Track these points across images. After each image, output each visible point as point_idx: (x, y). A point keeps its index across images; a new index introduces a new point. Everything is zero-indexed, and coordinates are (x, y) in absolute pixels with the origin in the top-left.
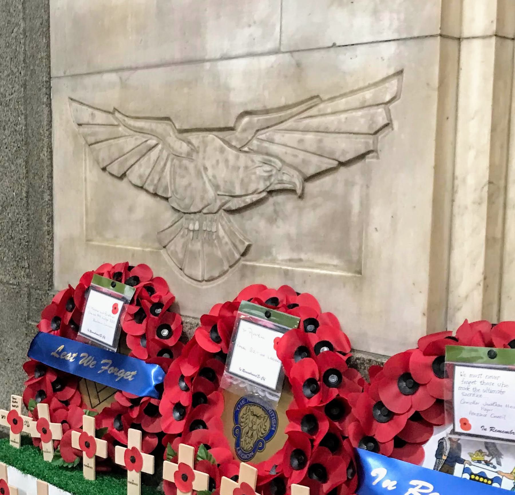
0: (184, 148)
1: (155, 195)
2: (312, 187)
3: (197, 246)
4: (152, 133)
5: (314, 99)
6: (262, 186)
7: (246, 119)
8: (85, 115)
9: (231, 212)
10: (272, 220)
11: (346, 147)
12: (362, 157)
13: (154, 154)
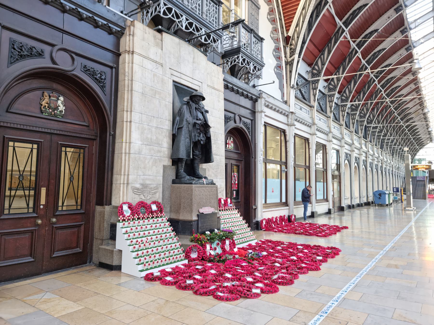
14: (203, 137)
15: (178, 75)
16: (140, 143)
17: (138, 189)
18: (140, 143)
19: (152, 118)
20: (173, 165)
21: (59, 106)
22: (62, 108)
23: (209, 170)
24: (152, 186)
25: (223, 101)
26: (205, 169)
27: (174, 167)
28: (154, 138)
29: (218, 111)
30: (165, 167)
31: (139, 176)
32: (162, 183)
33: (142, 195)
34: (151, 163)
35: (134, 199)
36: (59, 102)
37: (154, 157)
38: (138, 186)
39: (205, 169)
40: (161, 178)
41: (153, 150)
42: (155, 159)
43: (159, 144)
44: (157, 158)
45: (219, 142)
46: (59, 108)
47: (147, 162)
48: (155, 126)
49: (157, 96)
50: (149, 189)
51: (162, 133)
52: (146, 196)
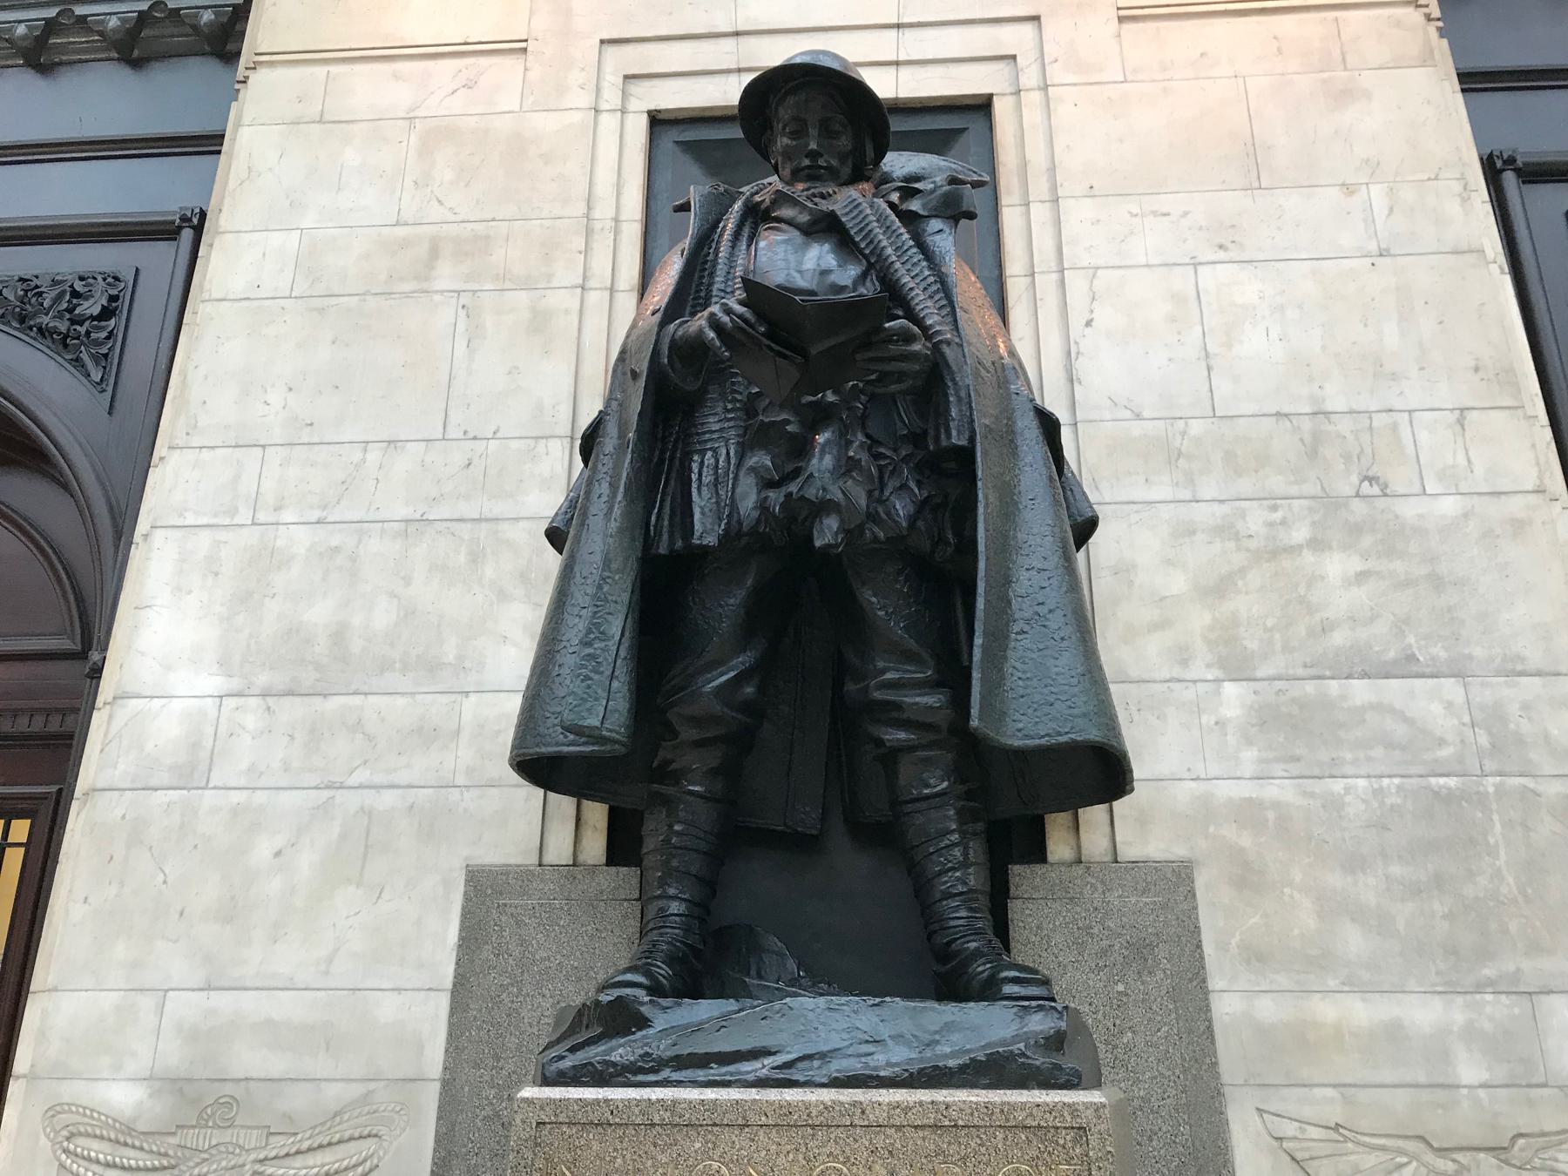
7: (1521, 1141)
14: (847, 467)
16: (213, 683)
18: (213, 683)
23: (1248, 878)
24: (297, 1101)
25: (1460, 96)
27: (627, 876)
28: (383, 616)
29: (1349, 189)
30: (484, 889)
31: (147, 1002)
34: (306, 861)
37: (352, 800)
38: (122, 1097)
41: (357, 726)
42: (367, 812)
43: (433, 667)
44: (388, 799)
47: (263, 849)
49: (446, 275)
50: (253, 1139)
51: (476, 558)
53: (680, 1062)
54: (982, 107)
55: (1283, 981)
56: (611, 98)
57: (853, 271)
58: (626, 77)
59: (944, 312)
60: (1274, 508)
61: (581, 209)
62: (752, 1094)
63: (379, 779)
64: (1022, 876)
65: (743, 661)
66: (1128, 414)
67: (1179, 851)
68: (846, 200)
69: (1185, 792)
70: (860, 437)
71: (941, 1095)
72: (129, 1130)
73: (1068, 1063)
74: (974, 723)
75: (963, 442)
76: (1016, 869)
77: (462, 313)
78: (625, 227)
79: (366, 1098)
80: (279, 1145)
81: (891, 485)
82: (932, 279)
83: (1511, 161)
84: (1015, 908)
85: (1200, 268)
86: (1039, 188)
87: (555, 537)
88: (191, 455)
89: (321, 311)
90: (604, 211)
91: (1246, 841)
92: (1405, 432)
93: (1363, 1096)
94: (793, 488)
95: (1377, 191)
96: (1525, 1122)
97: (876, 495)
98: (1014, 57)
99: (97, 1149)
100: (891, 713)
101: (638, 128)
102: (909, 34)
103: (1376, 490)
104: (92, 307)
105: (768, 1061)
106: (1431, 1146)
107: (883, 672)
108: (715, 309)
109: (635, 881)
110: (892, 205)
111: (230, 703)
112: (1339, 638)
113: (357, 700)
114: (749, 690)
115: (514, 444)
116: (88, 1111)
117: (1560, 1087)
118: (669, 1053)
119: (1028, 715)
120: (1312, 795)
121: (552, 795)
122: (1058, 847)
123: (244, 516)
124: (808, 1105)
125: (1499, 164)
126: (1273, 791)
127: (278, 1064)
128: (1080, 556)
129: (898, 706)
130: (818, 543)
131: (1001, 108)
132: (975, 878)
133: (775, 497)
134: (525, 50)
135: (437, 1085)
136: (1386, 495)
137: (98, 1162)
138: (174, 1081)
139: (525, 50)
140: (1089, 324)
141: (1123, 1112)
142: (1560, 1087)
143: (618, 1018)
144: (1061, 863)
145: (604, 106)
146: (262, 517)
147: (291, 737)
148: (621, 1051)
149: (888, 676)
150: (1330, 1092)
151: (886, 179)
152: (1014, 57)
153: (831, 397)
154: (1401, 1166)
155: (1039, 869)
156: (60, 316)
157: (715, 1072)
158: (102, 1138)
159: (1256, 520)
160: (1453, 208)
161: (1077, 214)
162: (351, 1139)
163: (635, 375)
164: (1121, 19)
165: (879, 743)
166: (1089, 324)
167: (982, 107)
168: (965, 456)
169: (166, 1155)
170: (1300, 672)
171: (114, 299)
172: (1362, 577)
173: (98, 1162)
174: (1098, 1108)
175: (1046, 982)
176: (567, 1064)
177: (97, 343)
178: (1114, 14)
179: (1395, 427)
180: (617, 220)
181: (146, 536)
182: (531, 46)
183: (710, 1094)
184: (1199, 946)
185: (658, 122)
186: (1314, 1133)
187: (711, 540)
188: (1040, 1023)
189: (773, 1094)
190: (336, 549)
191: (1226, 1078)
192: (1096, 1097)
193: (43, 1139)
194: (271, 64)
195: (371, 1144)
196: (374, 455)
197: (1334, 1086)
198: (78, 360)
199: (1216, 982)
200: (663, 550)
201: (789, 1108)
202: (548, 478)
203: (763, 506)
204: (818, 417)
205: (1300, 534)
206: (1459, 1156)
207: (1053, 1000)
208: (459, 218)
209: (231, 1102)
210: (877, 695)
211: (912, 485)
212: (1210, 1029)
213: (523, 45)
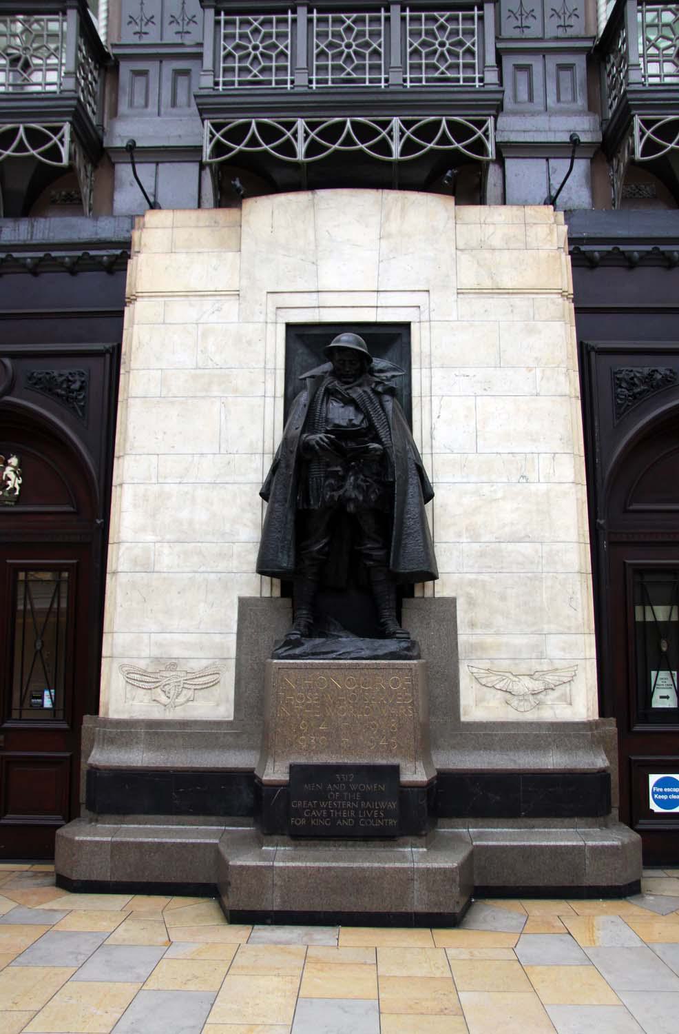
0: (517, 679)
1: (506, 691)
2: (556, 688)
3: (522, 703)
4: (504, 676)
5: (557, 669)
6: (543, 688)
8: (475, 670)
9: (533, 694)
10: (546, 695)
11: (566, 679)
12: (569, 681)
13: (505, 681)
15: (311, 300)
17: (144, 673)
19: (196, 458)
20: (284, 594)
21: (9, 479)
22: (14, 482)
26: (452, 602)
27: (287, 602)
29: (530, 369)
31: (145, 636)
32: (233, 652)
33: (159, 690)
35: (131, 702)
36: (9, 471)
38: (142, 664)
39: (452, 602)
40: (233, 639)
44: (213, 576)
45: (533, 487)
46: (9, 482)
48: (209, 480)
49: (216, 391)
50: (183, 674)
52: (171, 695)
53: (313, 654)
54: (406, 326)
55: (479, 631)
56: (271, 317)
57: (361, 417)
58: (278, 308)
59: (388, 433)
60: (492, 486)
61: (262, 365)
62: (332, 661)
63: (209, 570)
64: (406, 602)
65: (325, 541)
66: (448, 451)
67: (452, 595)
68: (357, 392)
69: (455, 577)
70: (362, 477)
71: (378, 661)
72: (145, 671)
73: (410, 653)
74: (391, 567)
75: (392, 480)
76: (405, 600)
77: (223, 405)
78: (278, 371)
79: (214, 664)
80: (190, 676)
81: (371, 490)
82: (384, 421)
83: (593, 348)
84: (404, 611)
85: (477, 397)
86: (426, 363)
87: (264, 495)
88: (133, 457)
89: (172, 403)
90: (270, 365)
91: (472, 591)
92: (536, 461)
93: (496, 662)
94: (341, 492)
95: (538, 371)
96: (539, 668)
97: (366, 495)
98: (419, 307)
99: (136, 676)
100: (369, 557)
101: (282, 331)
102: (382, 295)
103: (525, 481)
104: (76, 386)
105: (335, 654)
106: (512, 674)
107: (366, 544)
108: (318, 439)
109: (290, 602)
110: (374, 391)
111: (159, 544)
112: (507, 529)
113: (200, 544)
114: (327, 549)
115: (245, 456)
116: (134, 667)
117: (550, 659)
118: (310, 652)
119: (408, 565)
120: (493, 578)
121: (263, 576)
122: (418, 594)
123: (154, 480)
124: (345, 664)
125: (589, 348)
126: (481, 577)
127: (186, 654)
128: (428, 506)
129: (371, 555)
130: (348, 510)
131: (414, 328)
132: (393, 604)
133: (336, 495)
134: (239, 295)
135: (234, 660)
136: (527, 482)
137: (137, 680)
138: (157, 658)
139: (239, 295)
140: (439, 417)
141: (426, 667)
142: (550, 659)
143: (297, 644)
144: (417, 598)
145: (269, 321)
146: (161, 481)
147: (179, 557)
148: (297, 651)
149: (369, 546)
150: (487, 661)
151: (372, 372)
152: (419, 307)
153: (353, 463)
154: (503, 680)
155: (412, 600)
156: (64, 389)
157: (322, 657)
158: (137, 674)
159: (486, 489)
160: (562, 378)
161: (438, 373)
162: (211, 674)
163: (291, 452)
164: (458, 293)
165: (365, 565)
166: (439, 417)
167: (406, 326)
168: (393, 483)
169: (157, 678)
170: (494, 540)
171: (83, 382)
172: (517, 509)
173: (137, 680)
174: (415, 664)
175: (408, 633)
176: (284, 654)
177: (80, 401)
178: (456, 291)
179: (533, 459)
180: (275, 369)
181: (121, 485)
182: (241, 293)
183: (321, 661)
184: (456, 622)
185: (290, 327)
186: (482, 671)
187: (316, 507)
188: (404, 645)
189: (337, 661)
190: (187, 493)
191: (460, 657)
192: (415, 662)
193: (120, 675)
194: (142, 297)
195: (215, 677)
196: (196, 458)
197: (490, 659)
198: (74, 407)
199: (458, 633)
200: (300, 508)
201: (340, 665)
202: (258, 469)
203: (332, 497)
204: (347, 469)
205: (500, 495)
206: (520, 677)
207: (409, 638)
208: (218, 367)
209: (175, 664)
210: (365, 552)
211: (377, 490)
212: (457, 644)
213: (238, 293)
